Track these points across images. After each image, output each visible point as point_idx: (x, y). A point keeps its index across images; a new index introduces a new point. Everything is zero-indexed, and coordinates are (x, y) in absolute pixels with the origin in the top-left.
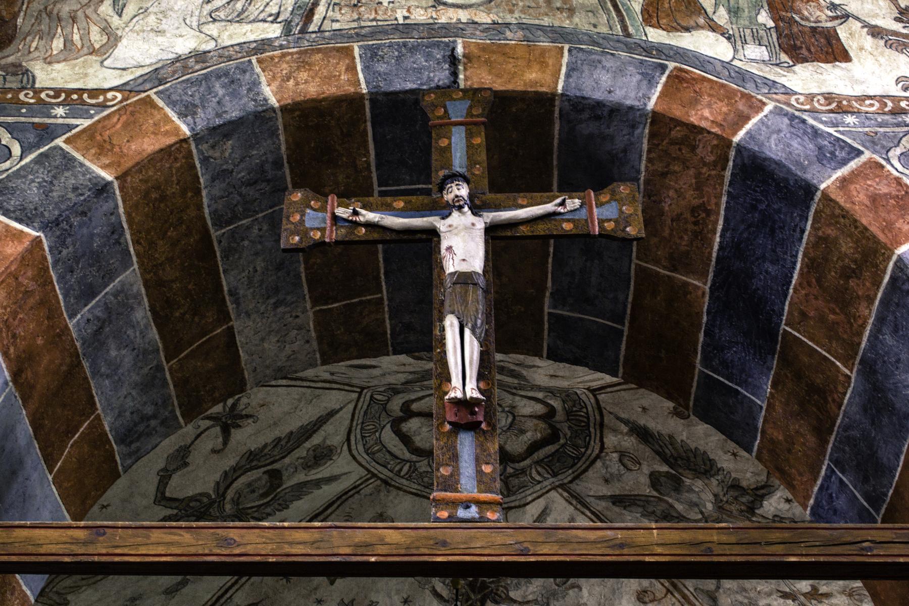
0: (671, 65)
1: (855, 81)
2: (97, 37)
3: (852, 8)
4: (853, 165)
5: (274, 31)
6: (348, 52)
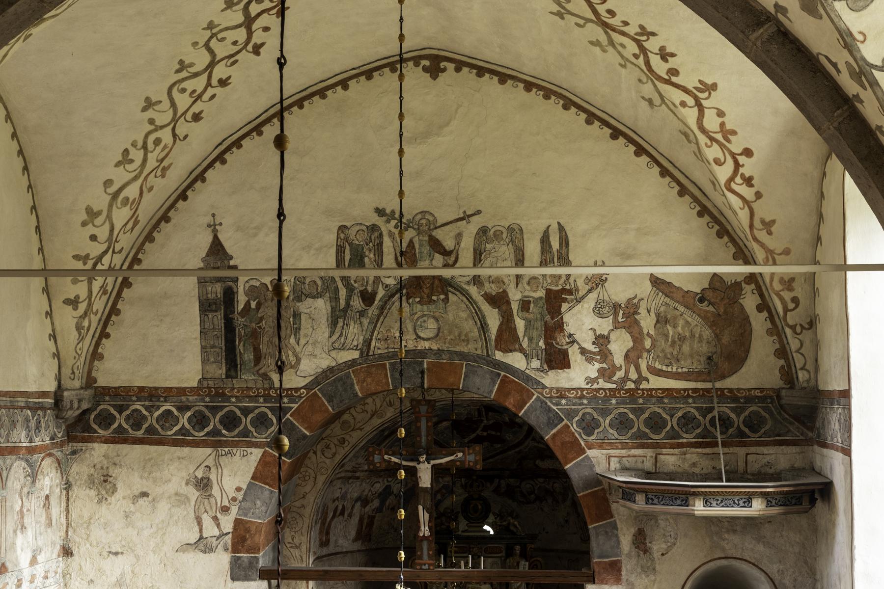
1: (570, 380)
2: (292, 359)
4: (559, 427)
6: (385, 365)
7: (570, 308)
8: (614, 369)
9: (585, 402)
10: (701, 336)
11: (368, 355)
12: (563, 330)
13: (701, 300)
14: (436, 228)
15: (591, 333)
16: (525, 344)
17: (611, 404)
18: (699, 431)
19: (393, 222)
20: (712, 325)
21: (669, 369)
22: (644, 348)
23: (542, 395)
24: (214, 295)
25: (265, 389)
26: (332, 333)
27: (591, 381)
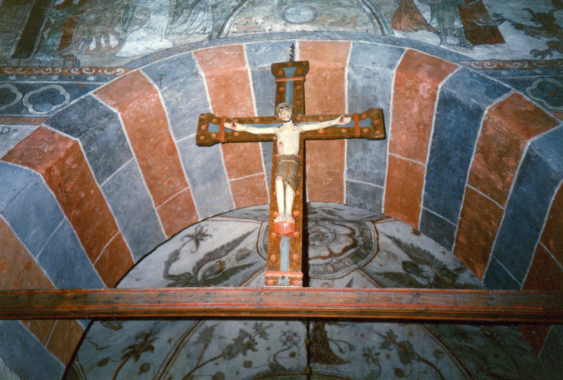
0: (407, 49)
3: (505, 16)
6: (241, 47)
23: (470, 66)
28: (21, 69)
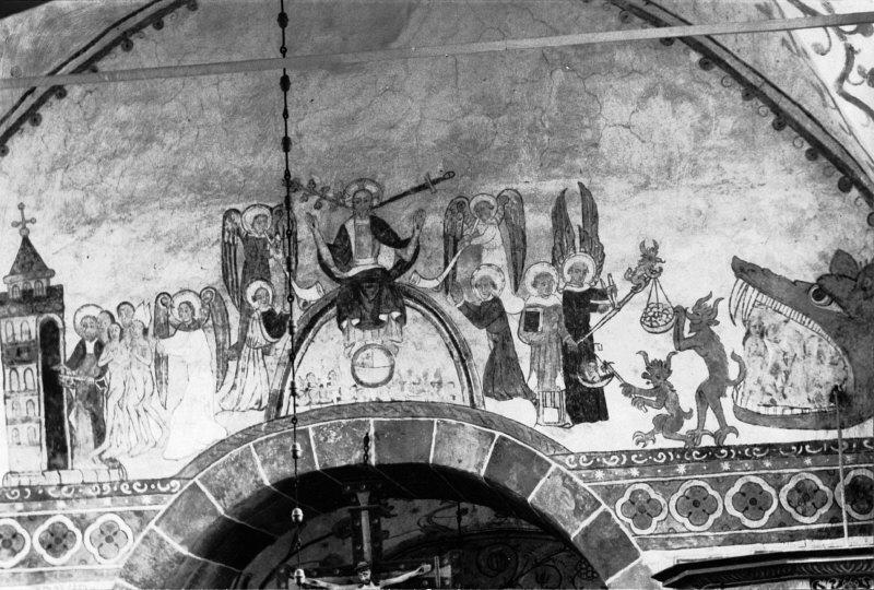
0: (498, 434)
3: (616, 367)
4: (594, 516)
5: (258, 418)
7: (603, 322)
8: (680, 417)
9: (634, 472)
10: (820, 354)
11: (277, 417)
12: (593, 357)
13: (818, 296)
14: (382, 204)
15: (640, 358)
16: (532, 383)
17: (678, 474)
18: (823, 511)
19: (314, 200)
20: (838, 335)
21: (771, 411)
22: (728, 380)
23: (564, 464)
24: (25, 338)
25: (112, 484)
26: (220, 385)
27: (641, 438)
28: (65, 489)
